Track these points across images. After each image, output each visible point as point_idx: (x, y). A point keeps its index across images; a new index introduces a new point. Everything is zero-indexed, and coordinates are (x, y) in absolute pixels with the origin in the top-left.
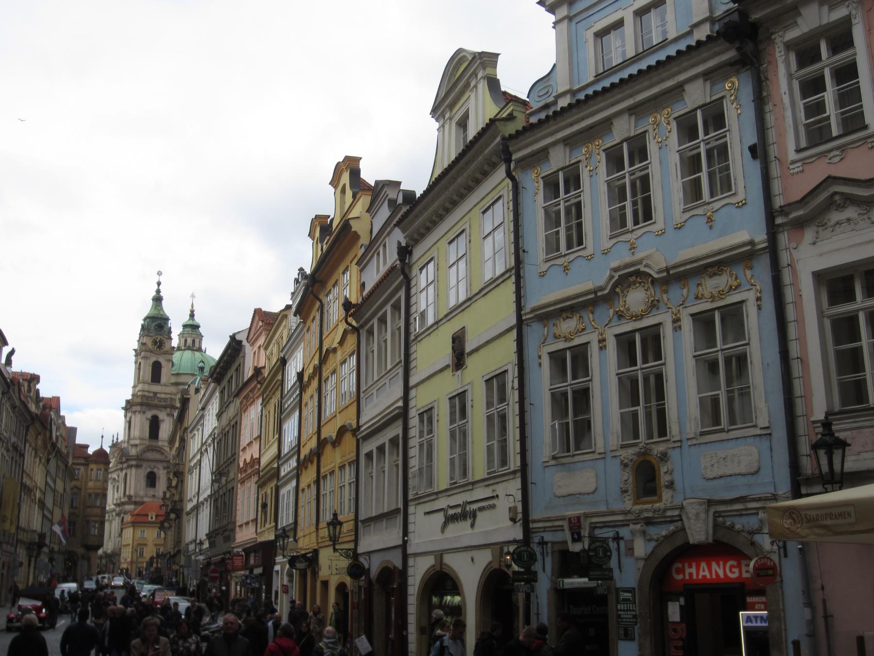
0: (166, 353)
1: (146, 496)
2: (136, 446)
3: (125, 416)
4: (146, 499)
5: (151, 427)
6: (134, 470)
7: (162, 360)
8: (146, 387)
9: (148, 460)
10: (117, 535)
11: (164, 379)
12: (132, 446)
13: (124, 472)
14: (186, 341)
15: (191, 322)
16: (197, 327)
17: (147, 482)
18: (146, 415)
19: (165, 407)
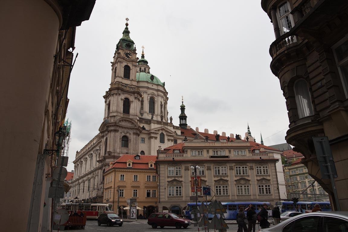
0: (133, 61)
1: (122, 153)
2: (114, 116)
3: (106, 102)
4: (121, 155)
5: (124, 105)
6: (112, 134)
7: (130, 65)
8: (120, 80)
9: (122, 127)
10: (99, 183)
11: (132, 77)
12: (111, 117)
13: (105, 138)
14: (140, 69)
15: (143, 59)
16: (146, 62)
17: (122, 143)
18: (120, 98)
19: (134, 93)
